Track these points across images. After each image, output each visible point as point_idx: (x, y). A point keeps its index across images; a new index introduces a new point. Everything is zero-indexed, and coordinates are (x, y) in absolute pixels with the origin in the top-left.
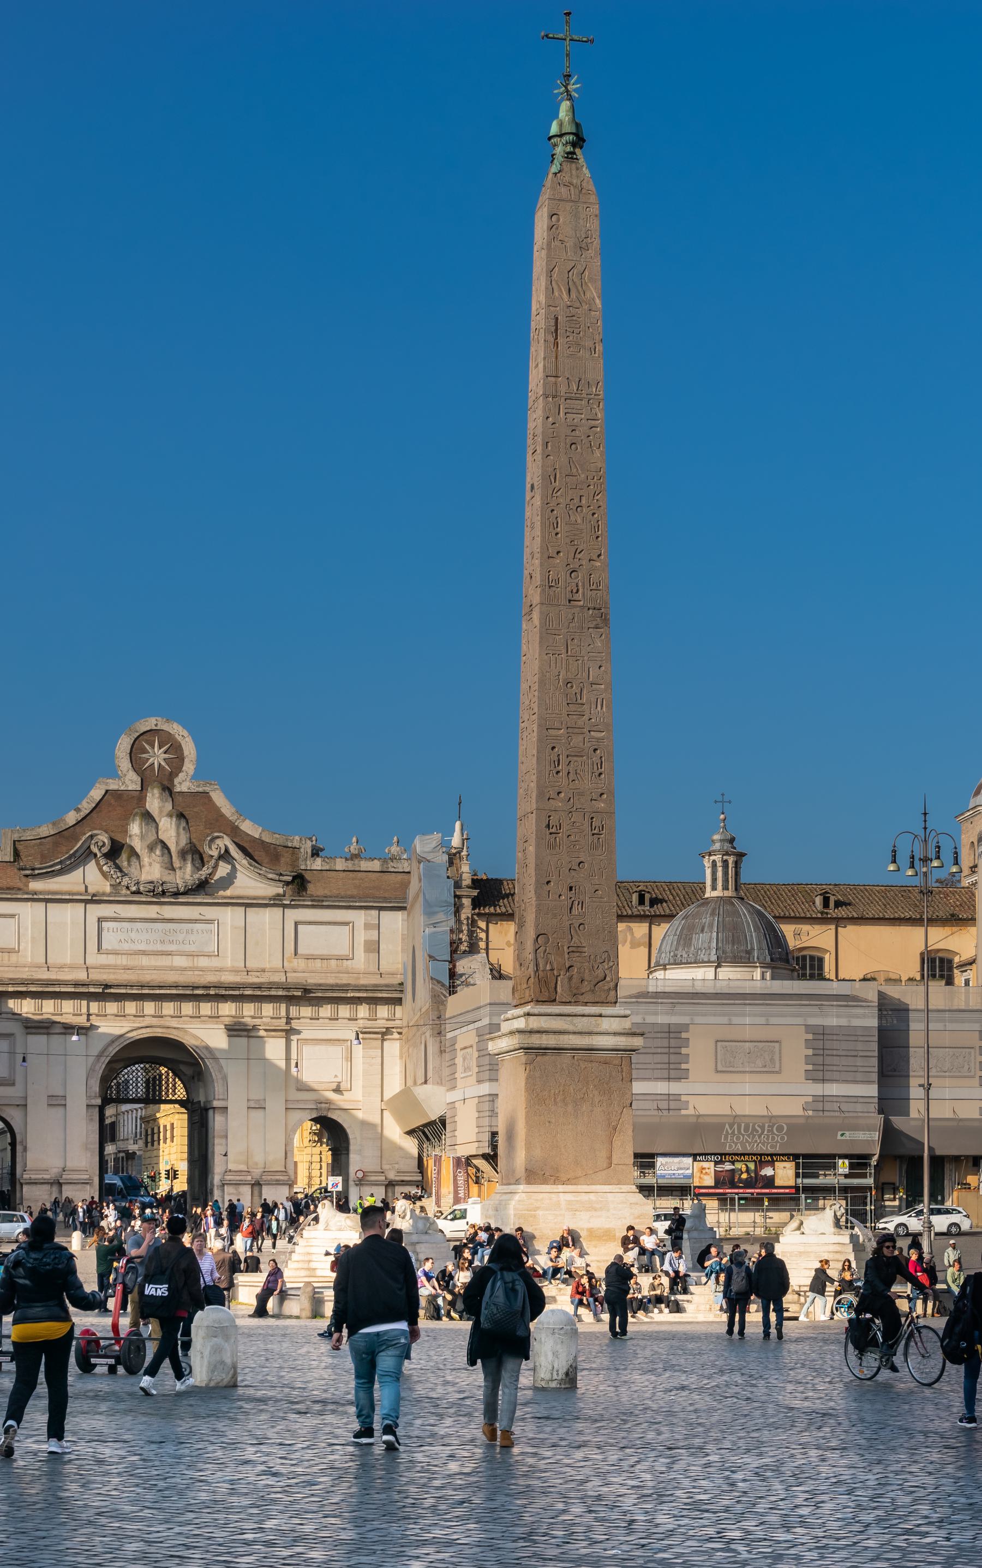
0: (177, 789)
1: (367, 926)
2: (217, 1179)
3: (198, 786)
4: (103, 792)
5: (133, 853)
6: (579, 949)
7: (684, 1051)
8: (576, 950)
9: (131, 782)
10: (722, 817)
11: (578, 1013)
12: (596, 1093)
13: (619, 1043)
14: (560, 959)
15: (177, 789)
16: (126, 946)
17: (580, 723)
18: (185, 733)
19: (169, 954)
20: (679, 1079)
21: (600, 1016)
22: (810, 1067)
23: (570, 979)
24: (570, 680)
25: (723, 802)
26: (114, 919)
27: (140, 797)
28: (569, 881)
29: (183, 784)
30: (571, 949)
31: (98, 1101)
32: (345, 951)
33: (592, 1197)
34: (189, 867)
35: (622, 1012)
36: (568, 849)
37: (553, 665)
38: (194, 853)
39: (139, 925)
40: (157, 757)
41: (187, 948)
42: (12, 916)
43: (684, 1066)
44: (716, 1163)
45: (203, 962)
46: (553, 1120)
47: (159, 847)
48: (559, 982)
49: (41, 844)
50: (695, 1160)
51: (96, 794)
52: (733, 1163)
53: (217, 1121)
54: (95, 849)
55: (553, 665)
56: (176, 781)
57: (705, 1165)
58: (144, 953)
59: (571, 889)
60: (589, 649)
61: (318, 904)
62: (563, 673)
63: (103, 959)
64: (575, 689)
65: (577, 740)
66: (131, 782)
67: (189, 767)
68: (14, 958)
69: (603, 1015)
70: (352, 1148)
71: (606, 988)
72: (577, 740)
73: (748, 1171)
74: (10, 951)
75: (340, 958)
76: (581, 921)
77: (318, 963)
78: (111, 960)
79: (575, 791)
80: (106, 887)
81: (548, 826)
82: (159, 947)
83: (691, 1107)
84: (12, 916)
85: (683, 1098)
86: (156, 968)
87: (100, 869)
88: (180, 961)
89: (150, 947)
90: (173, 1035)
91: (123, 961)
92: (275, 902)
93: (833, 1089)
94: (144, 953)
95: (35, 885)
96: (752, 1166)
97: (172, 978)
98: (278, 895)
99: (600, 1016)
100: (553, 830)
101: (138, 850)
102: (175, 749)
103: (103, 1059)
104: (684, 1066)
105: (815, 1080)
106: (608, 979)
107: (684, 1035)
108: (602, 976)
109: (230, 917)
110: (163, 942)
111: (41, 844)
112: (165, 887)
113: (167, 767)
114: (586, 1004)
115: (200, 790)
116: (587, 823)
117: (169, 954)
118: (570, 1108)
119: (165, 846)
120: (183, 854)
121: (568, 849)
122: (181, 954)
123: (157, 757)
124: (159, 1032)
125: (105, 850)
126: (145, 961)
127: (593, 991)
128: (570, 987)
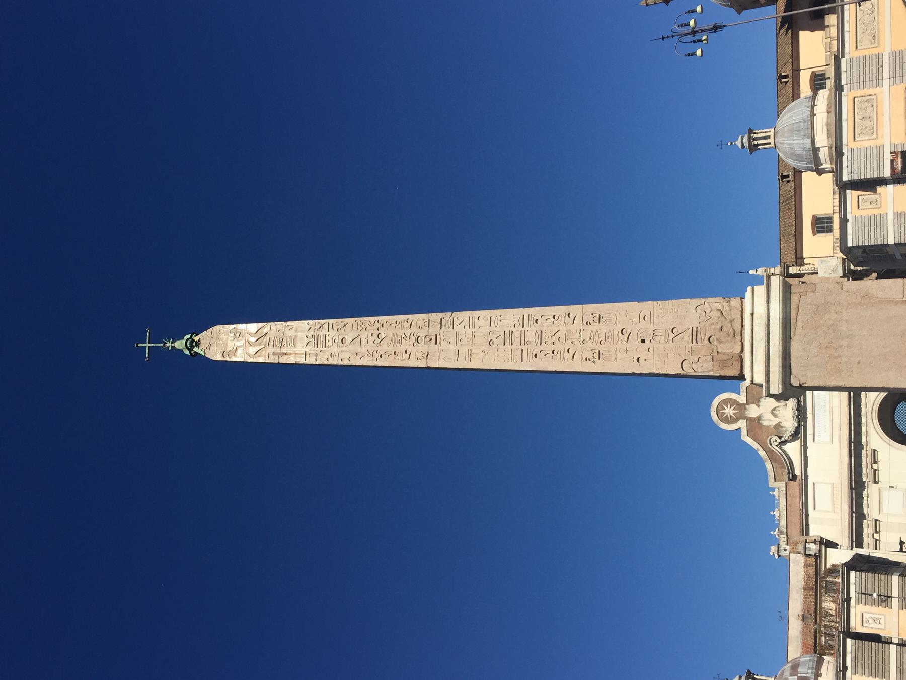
3: (743, 392)
4: (748, 437)
5: (778, 426)
6: (694, 333)
9: (742, 424)
10: (729, 144)
11: (750, 335)
12: (827, 317)
13: (777, 298)
14: (703, 351)
15: (746, 403)
17: (517, 334)
18: (717, 398)
21: (752, 314)
23: (720, 341)
24: (488, 343)
25: (721, 145)
27: (750, 420)
28: (637, 343)
29: (742, 399)
30: (694, 341)
36: (612, 344)
42: (814, 484)
46: (857, 360)
47: (774, 412)
48: (723, 351)
49: (776, 468)
51: (749, 441)
56: (741, 403)
58: (832, 420)
59: (643, 341)
60: (467, 327)
62: (483, 348)
64: (494, 339)
65: (530, 336)
66: (742, 424)
69: (751, 312)
71: (728, 308)
72: (530, 336)
76: (670, 332)
79: (567, 339)
81: (594, 362)
82: (828, 412)
84: (814, 484)
91: (836, 432)
94: (832, 420)
95: (798, 472)
99: (752, 314)
100: (597, 355)
101: (777, 422)
102: (726, 402)
103: (891, 443)
108: (719, 314)
110: (825, 411)
111: (776, 468)
112: (795, 408)
113: (734, 406)
115: (745, 391)
116: (590, 328)
118: (844, 343)
119: (774, 409)
121: (612, 344)
123: (729, 411)
124: (875, 415)
125: (777, 438)
127: (731, 321)
128: (728, 341)
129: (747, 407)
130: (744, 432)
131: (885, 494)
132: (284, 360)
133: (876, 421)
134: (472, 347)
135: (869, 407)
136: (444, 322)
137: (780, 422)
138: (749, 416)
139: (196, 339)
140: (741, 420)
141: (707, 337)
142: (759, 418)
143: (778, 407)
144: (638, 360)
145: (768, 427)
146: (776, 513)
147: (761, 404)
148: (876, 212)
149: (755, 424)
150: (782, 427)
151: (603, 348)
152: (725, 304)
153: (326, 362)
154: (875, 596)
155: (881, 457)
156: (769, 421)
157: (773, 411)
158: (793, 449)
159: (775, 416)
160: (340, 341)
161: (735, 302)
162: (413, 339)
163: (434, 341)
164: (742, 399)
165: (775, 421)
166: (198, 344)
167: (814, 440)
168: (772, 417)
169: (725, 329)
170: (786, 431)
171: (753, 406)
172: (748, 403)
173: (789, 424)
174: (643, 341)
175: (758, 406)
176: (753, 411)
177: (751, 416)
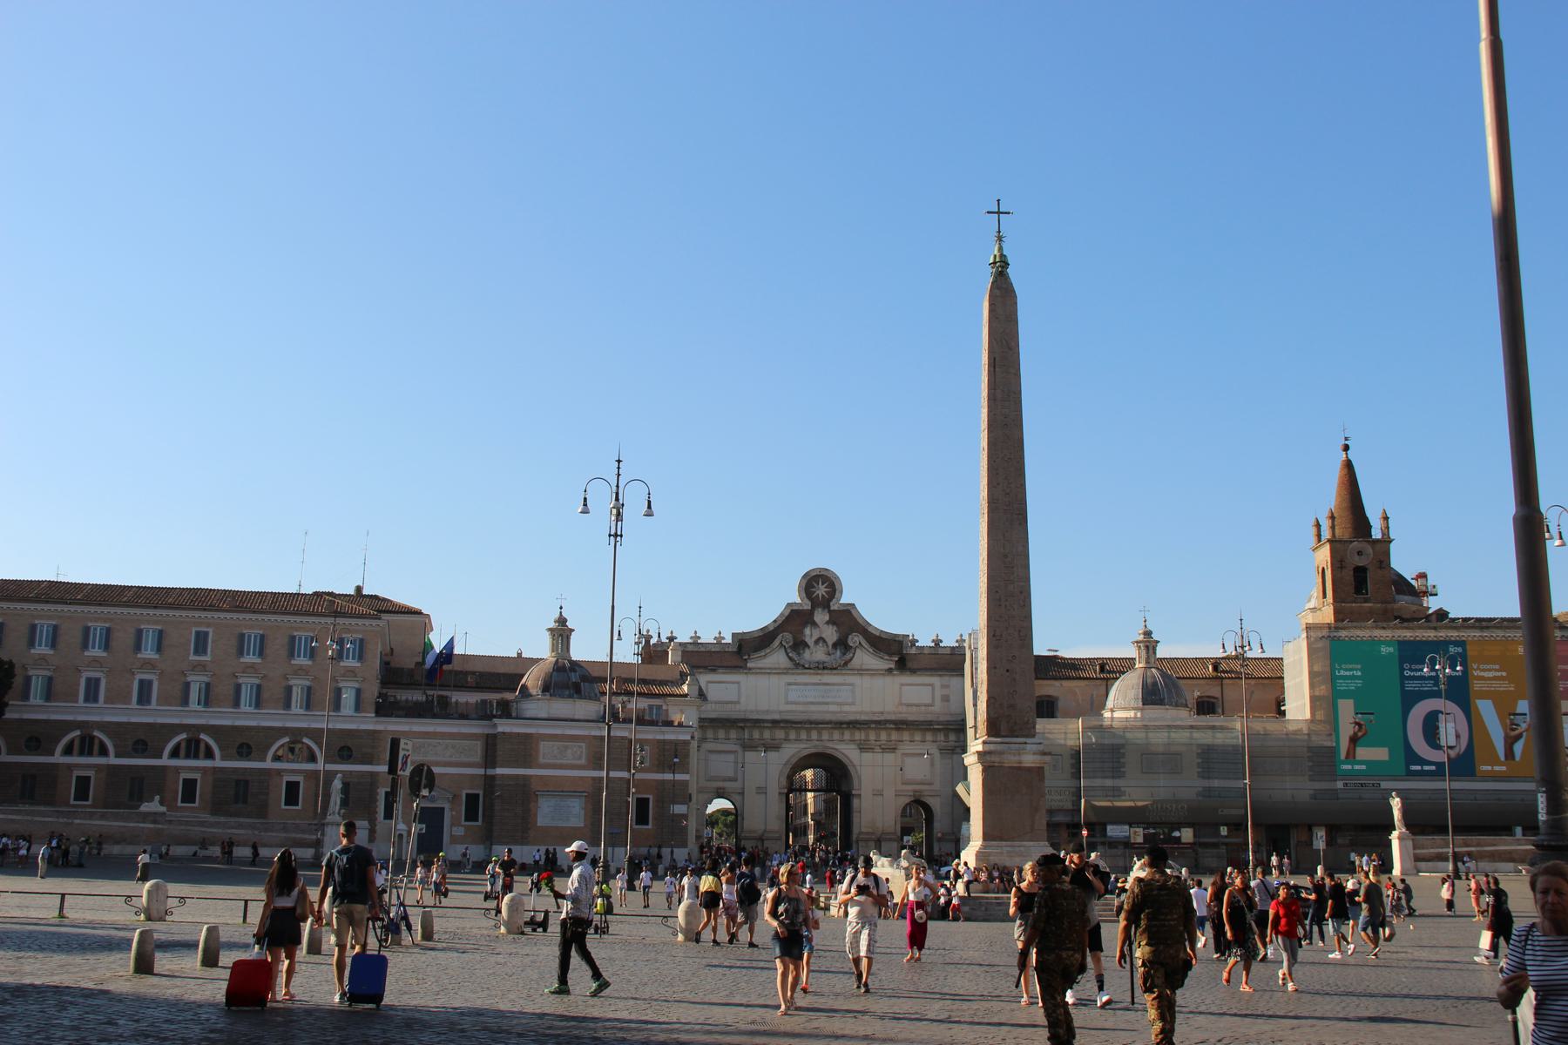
0: (832, 609)
1: (943, 686)
2: (854, 837)
5: (806, 645)
7: (1122, 760)
8: (1012, 706)
15: (832, 609)
16: (801, 699)
19: (827, 704)
20: (1119, 777)
21: (1026, 743)
22: (1200, 770)
26: (796, 684)
27: (811, 613)
29: (834, 606)
31: (786, 791)
32: (928, 701)
33: (1022, 849)
34: (838, 652)
35: (1039, 741)
38: (842, 644)
39: (809, 687)
41: (839, 700)
42: (738, 683)
43: (1122, 770)
44: (1144, 829)
45: (846, 708)
50: (1131, 826)
52: (1154, 828)
53: (855, 802)
56: (831, 604)
57: (1137, 830)
59: (1008, 671)
61: (914, 671)
63: (789, 707)
68: (738, 707)
70: (935, 819)
73: (1164, 833)
74: (735, 703)
75: (926, 705)
77: (914, 709)
78: (793, 707)
80: (788, 664)
81: (994, 636)
82: (821, 700)
83: (1127, 794)
85: (1122, 789)
86: (819, 712)
87: (787, 654)
88: (832, 708)
89: (817, 700)
91: (800, 708)
92: (890, 671)
93: (1216, 783)
94: (812, 703)
96: (1166, 830)
97: (828, 717)
98: (891, 669)
99: (1026, 743)
104: (1122, 770)
105: (1203, 778)
107: (1122, 751)
109: (866, 682)
114: (1017, 737)
117: (827, 704)
119: (825, 641)
120: (835, 645)
122: (833, 703)
124: (820, 750)
125: (790, 644)
126: (813, 708)
129: (826, 610)
131: (731, 757)
133: (813, 751)
136: (1020, 516)
137: (809, 647)
138: (816, 612)
140: (810, 603)
142: (814, 624)
143: (827, 645)
144: (995, 668)
145: (802, 633)
147: (831, 626)
150: (804, 652)
154: (675, 760)
155: (772, 755)
156: (809, 634)
157: (821, 640)
158: (777, 657)
159: (817, 642)
162: (1008, 491)
164: (834, 606)
165: (810, 641)
167: (790, 684)
168: (815, 638)
170: (799, 654)
171: (827, 618)
172: (830, 611)
174: (1008, 671)
175: (828, 623)
176: (821, 617)
177: (815, 614)
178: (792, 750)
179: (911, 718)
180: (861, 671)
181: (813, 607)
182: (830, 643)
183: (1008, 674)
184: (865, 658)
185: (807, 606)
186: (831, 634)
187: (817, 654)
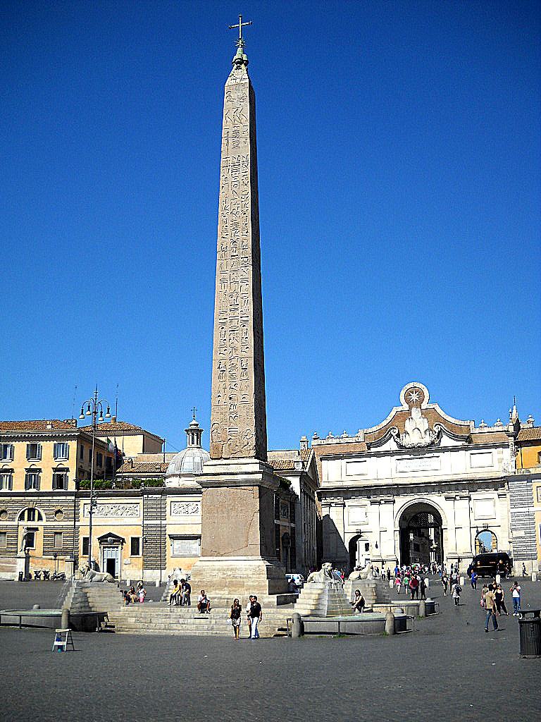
5: (406, 433)
29: (424, 405)
37: (223, 287)
40: (414, 397)
51: (393, 413)
54: (392, 433)
55: (223, 287)
59: (230, 398)
67: (426, 399)
90: (426, 501)
95: (373, 450)
106: (249, 444)
116: (239, 364)
123: (414, 397)
130: (400, 409)
131: (363, 510)
132: (224, 141)
134: (229, 283)
135: (425, 497)
136: (246, 259)
139: (243, 66)
141: (232, 438)
144: (219, 396)
146: (344, 435)
148: (535, 499)
149: (407, 415)
151: (227, 372)
152: (251, 447)
153: (221, 175)
155: (390, 506)
156: (409, 426)
158: (391, 445)
160: (236, 183)
161: (253, 453)
163: (235, 254)
166: (238, 68)
169: (237, 447)
173: (408, 441)
174: (230, 398)
176: (416, 413)
178: (402, 501)
179: (478, 476)
180: (445, 449)
181: (410, 408)
182: (423, 431)
183: (230, 401)
184: (446, 441)
185: (406, 407)
186: (424, 425)
187: (412, 439)
